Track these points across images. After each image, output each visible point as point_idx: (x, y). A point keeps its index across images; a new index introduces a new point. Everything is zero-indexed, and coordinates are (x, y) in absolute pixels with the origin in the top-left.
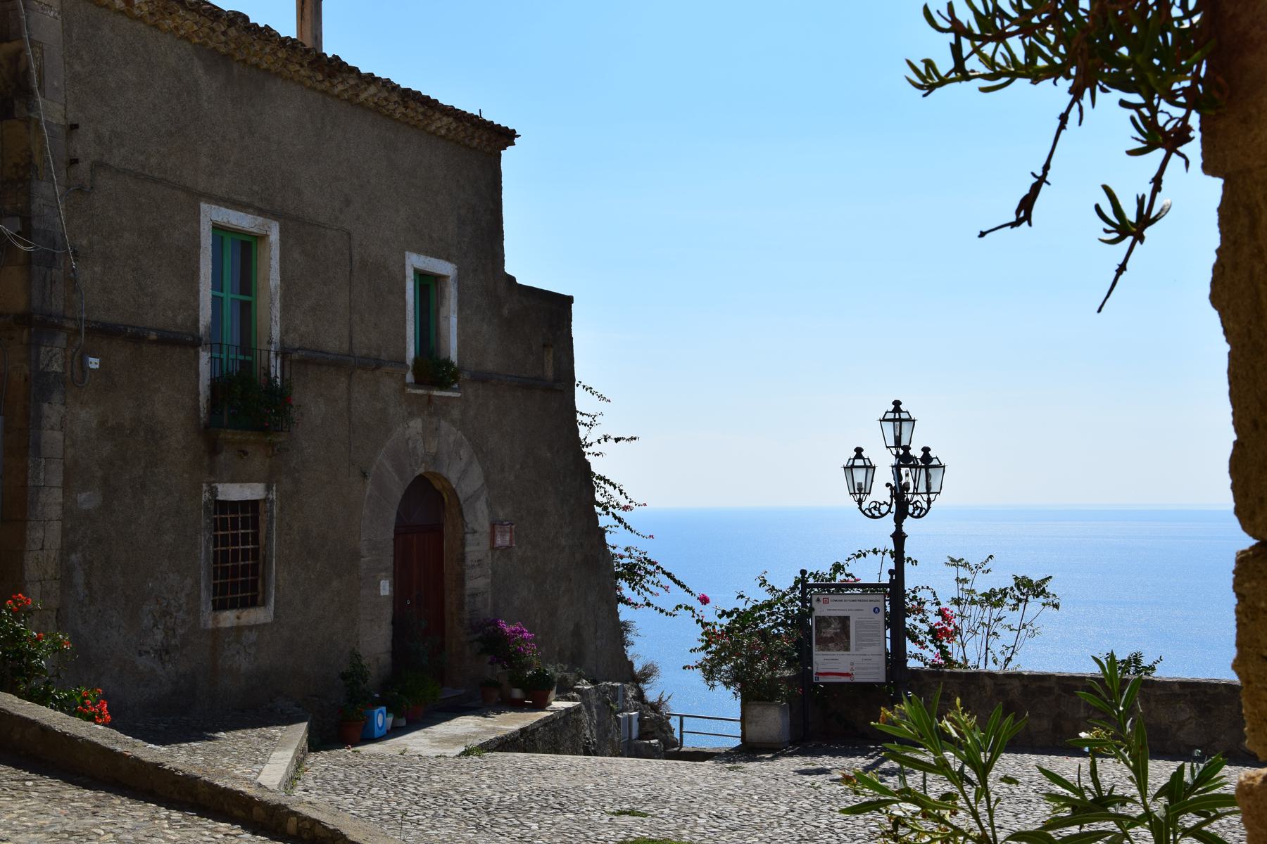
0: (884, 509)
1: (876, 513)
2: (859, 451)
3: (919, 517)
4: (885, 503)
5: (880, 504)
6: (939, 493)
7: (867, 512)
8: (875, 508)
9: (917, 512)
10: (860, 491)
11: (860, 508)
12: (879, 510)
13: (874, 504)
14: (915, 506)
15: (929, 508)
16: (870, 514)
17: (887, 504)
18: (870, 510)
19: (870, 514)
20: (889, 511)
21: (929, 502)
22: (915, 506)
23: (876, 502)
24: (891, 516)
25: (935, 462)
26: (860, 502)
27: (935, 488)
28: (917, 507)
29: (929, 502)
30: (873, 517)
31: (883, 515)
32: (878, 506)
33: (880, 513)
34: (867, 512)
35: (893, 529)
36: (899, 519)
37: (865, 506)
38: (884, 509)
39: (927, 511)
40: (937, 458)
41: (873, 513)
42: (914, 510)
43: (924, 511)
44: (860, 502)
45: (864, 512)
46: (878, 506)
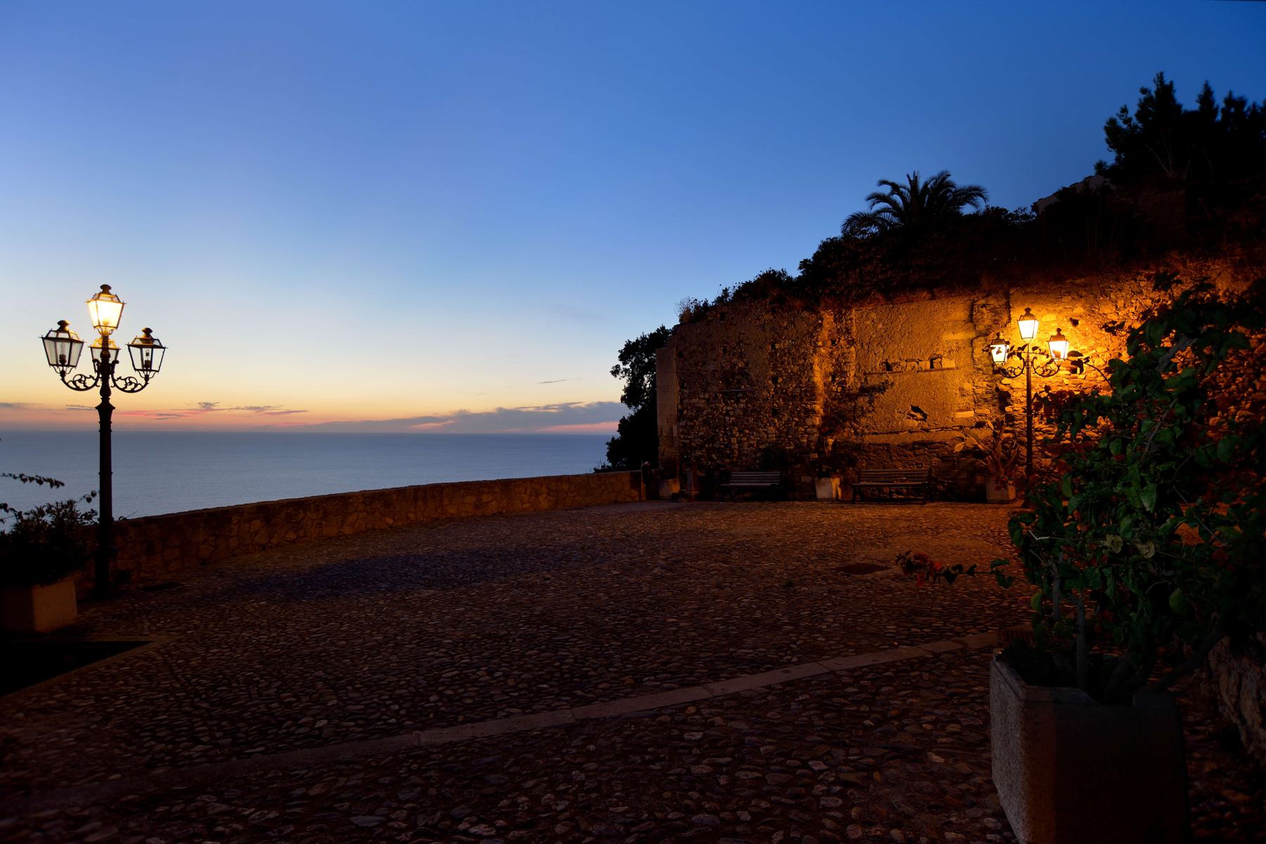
0: (90, 382)
1: (81, 386)
2: (63, 324)
3: (132, 391)
4: (91, 377)
5: (86, 378)
6: (158, 371)
7: (71, 384)
8: (80, 381)
9: (129, 388)
10: (62, 363)
11: (63, 380)
12: (84, 383)
13: (79, 377)
14: (128, 381)
15: (146, 384)
16: (74, 387)
17: (93, 378)
18: (74, 382)
19: (74, 387)
20: (95, 384)
21: (147, 378)
22: (128, 381)
23: (81, 375)
24: (97, 390)
25: (156, 343)
26: (63, 374)
27: (155, 367)
28: (131, 383)
29: (147, 378)
30: (78, 389)
31: (87, 388)
32: (83, 379)
33: (85, 386)
34: (71, 384)
35: (100, 401)
36: (105, 392)
37: (67, 378)
38: (90, 382)
39: (143, 387)
40: (158, 340)
41: (79, 385)
42: (126, 385)
43: (139, 387)
44: (63, 374)
45: (67, 384)
46: (83, 379)
